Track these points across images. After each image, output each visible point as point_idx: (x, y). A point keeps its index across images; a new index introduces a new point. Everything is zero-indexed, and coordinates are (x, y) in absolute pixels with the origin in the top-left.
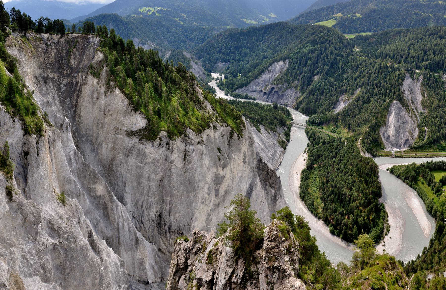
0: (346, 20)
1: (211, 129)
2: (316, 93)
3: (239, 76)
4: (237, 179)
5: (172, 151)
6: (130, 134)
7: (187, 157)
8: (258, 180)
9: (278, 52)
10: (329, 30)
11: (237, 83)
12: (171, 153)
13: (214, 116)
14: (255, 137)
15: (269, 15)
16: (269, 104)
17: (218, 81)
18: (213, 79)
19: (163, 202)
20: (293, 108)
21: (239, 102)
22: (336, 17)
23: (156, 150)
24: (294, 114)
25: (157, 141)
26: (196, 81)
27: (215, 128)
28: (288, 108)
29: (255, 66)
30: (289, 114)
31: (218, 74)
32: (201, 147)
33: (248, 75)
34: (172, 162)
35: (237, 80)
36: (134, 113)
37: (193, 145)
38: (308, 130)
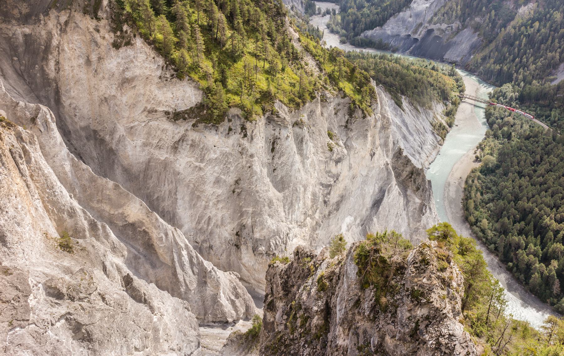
1: (317, 102)
2: (517, 42)
4: (359, 179)
5: (252, 139)
7: (277, 147)
8: (394, 182)
12: (251, 142)
13: (320, 79)
19: (242, 215)
23: (223, 138)
25: (226, 125)
26: (287, 18)
27: (324, 100)
32: (300, 130)
34: (252, 156)
35: (362, 15)
36: (178, 81)
37: (286, 127)
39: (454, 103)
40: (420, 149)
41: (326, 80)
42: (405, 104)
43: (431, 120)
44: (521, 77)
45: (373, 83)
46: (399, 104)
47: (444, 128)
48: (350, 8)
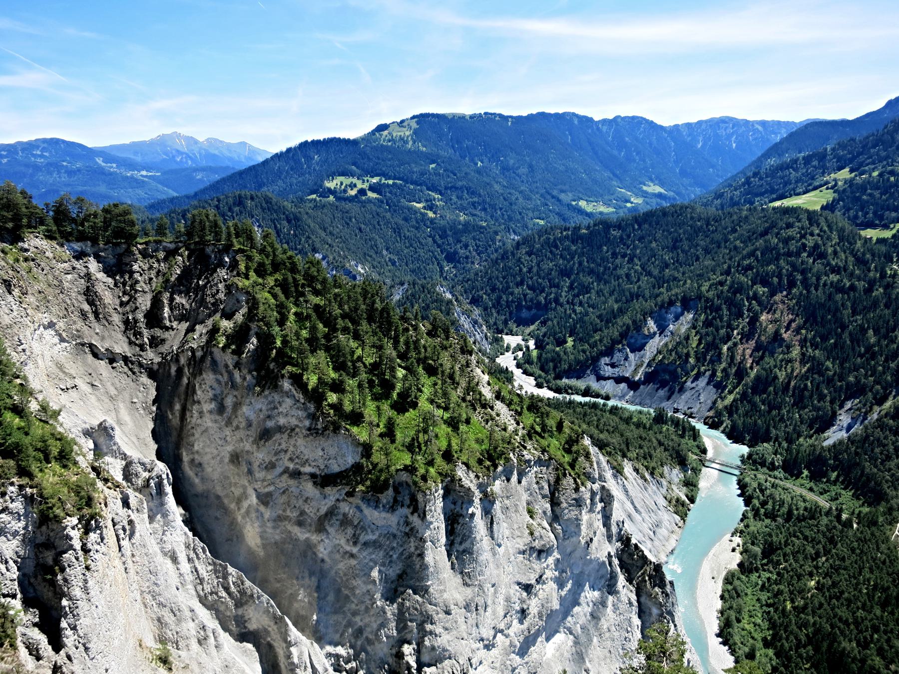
0: (863, 188)
3: (570, 342)
6: (324, 480)
9: (668, 282)
10: (812, 216)
11: (565, 357)
14: (612, 485)
15: (645, 188)
16: (645, 410)
17: (520, 354)
18: (508, 349)
20: (705, 424)
21: (571, 402)
22: (835, 180)
24: (709, 437)
28: (693, 422)
29: (609, 318)
30: (695, 435)
31: (520, 337)
33: (592, 340)
38: (747, 480)
39: (694, 470)
40: (652, 533)
41: (524, 436)
42: (628, 468)
43: (664, 491)
44: (781, 434)
45: (587, 441)
46: (618, 471)
47: (683, 504)
48: (548, 344)
